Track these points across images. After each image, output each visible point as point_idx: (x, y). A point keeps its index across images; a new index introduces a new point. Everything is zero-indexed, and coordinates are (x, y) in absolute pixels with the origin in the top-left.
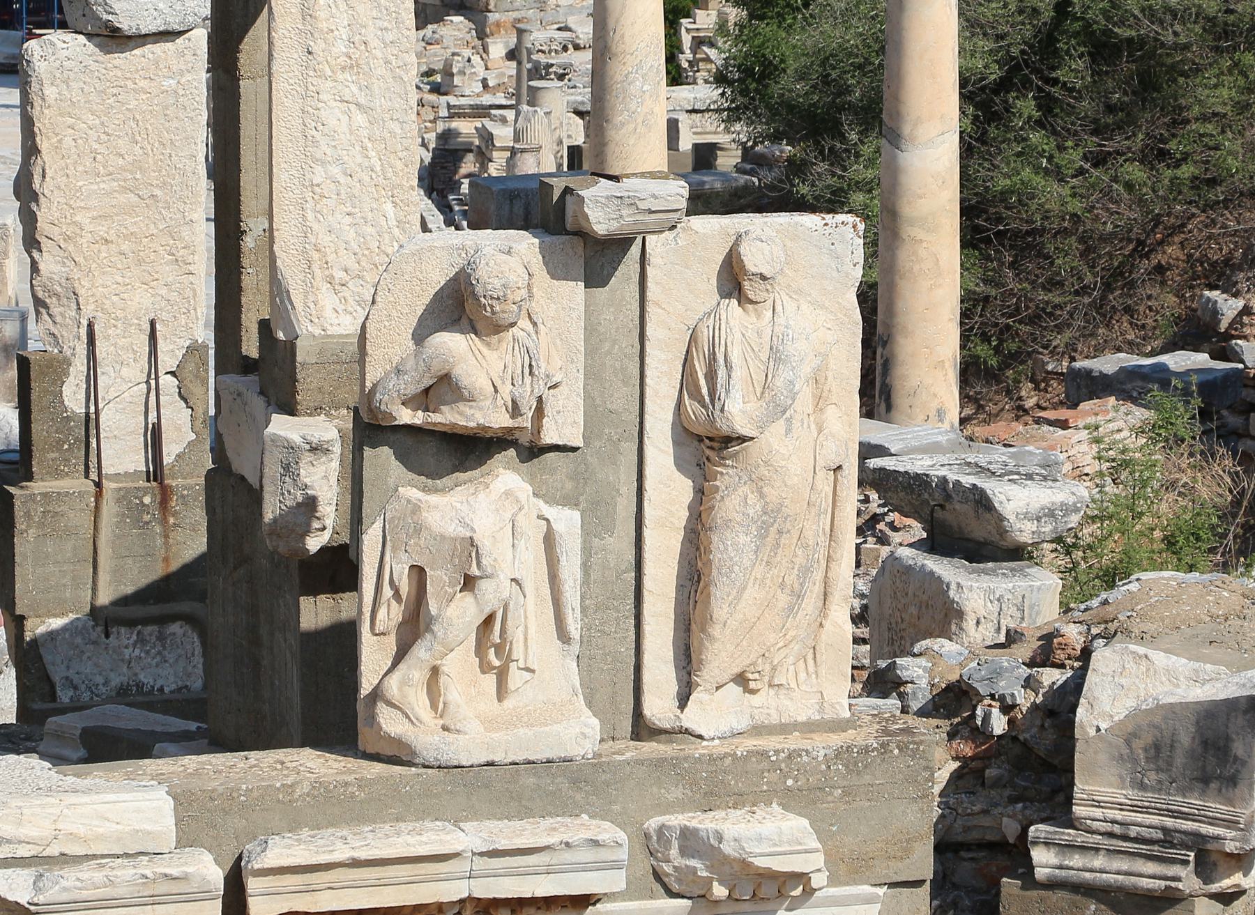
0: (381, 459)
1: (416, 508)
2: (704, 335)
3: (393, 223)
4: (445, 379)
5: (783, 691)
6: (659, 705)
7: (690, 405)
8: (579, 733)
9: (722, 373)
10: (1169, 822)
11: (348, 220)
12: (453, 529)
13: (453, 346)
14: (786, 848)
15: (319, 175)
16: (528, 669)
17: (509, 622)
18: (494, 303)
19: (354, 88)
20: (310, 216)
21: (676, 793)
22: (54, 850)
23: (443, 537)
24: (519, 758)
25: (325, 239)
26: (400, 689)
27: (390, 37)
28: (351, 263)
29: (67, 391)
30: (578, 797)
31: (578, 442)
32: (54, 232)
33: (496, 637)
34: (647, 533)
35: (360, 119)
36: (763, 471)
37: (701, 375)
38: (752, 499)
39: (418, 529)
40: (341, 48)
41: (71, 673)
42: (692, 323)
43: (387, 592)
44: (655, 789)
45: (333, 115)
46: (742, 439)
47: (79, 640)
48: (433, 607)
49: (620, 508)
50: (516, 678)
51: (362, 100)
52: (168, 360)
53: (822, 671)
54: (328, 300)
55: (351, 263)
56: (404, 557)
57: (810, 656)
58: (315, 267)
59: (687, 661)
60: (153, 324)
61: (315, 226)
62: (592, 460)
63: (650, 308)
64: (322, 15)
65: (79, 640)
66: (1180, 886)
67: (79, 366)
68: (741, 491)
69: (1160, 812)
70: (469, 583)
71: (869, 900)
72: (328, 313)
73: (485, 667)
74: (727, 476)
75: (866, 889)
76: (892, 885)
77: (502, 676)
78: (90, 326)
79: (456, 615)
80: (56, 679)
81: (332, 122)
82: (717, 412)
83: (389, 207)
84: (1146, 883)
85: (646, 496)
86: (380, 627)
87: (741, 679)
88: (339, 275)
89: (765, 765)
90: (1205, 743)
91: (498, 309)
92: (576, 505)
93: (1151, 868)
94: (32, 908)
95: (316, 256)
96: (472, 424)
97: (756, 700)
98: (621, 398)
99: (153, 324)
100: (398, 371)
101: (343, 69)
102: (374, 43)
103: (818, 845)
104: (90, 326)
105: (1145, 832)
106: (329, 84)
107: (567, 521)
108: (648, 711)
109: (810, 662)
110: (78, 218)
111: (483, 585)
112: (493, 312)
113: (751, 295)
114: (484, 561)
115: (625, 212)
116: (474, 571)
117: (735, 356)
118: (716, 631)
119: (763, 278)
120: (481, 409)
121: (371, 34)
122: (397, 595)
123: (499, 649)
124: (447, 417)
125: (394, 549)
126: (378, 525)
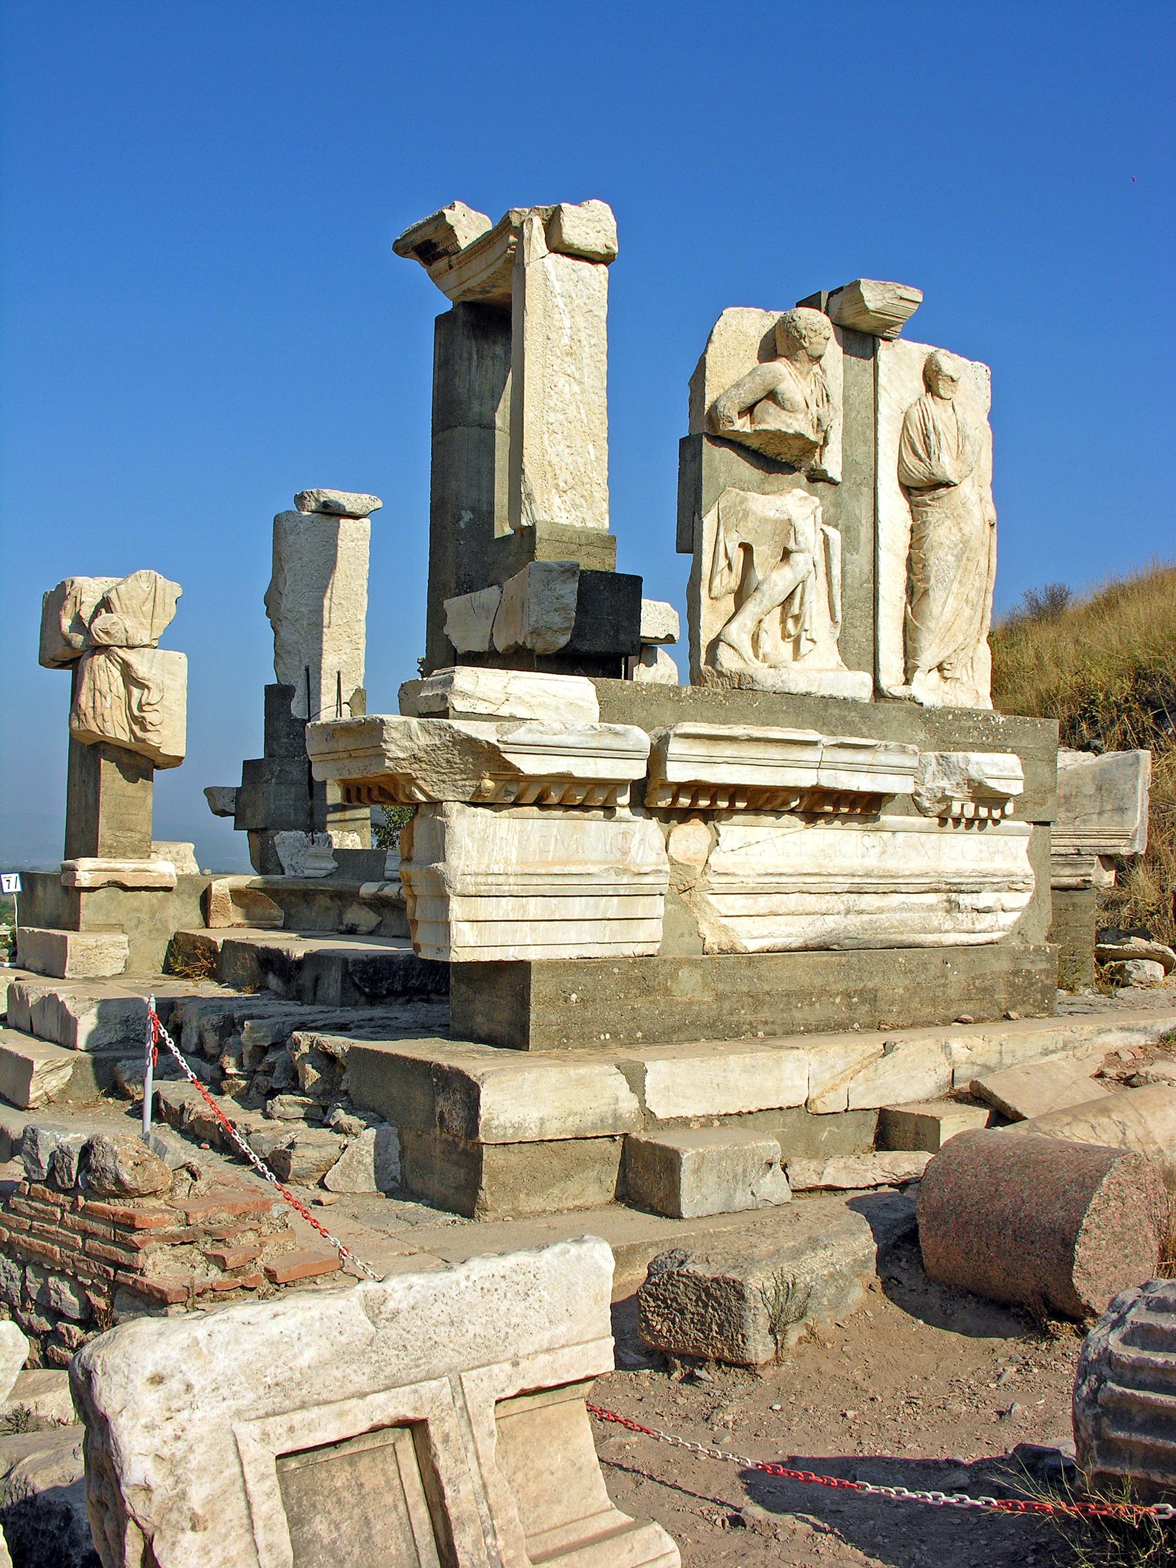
0: (718, 461)
1: (743, 500)
2: (916, 415)
3: (593, 458)
4: (772, 396)
5: (958, 685)
6: (891, 680)
7: (910, 459)
8: (858, 685)
9: (933, 437)
10: (1077, 842)
11: (568, 450)
12: (772, 514)
13: (780, 366)
14: (1005, 774)
15: (552, 417)
16: (812, 640)
17: (806, 597)
18: (812, 334)
19: (573, 367)
20: (546, 443)
21: (922, 736)
22: (504, 711)
23: (766, 520)
24: (827, 693)
25: (555, 460)
26: (738, 634)
27: (593, 342)
28: (570, 480)
29: (293, 704)
30: (864, 730)
31: (839, 478)
32: (289, 615)
33: (795, 610)
34: (881, 553)
35: (576, 388)
36: (961, 511)
37: (919, 440)
38: (955, 530)
39: (746, 514)
40: (566, 340)
41: (293, 863)
42: (905, 409)
43: (722, 562)
44: (909, 731)
45: (561, 381)
46: (948, 485)
47: (297, 844)
48: (759, 573)
49: (862, 534)
50: (805, 646)
51: (577, 376)
52: (346, 697)
53: (976, 675)
54: (557, 501)
55: (570, 480)
56: (735, 536)
57: (969, 665)
58: (549, 476)
59: (909, 653)
60: (339, 673)
61: (549, 450)
62: (845, 495)
63: (880, 390)
64: (557, 316)
65: (297, 844)
66: (1091, 878)
67: (300, 693)
68: (948, 523)
69: (1070, 836)
70: (786, 554)
71: (1022, 834)
72: (555, 508)
73: (785, 635)
74: (934, 515)
75: (1023, 824)
76: (1035, 823)
77: (797, 642)
78: (307, 670)
79: (776, 581)
80: (285, 865)
81: (560, 385)
82: (933, 463)
83: (590, 447)
84: (1066, 881)
85: (880, 526)
86: (714, 593)
87: (940, 668)
88: (562, 484)
89: (971, 723)
90: (1099, 789)
91: (813, 340)
92: (836, 526)
93: (1068, 871)
94: (501, 746)
95: (549, 469)
96: (791, 431)
97: (946, 687)
98: (861, 453)
99: (339, 673)
100: (737, 385)
101: (567, 354)
102: (585, 343)
103: (1020, 774)
104: (307, 670)
105: (1062, 851)
106: (559, 361)
107: (835, 535)
108: (884, 683)
109: (970, 669)
110: (302, 609)
111: (795, 557)
112: (811, 343)
113: (942, 392)
114: (800, 538)
115: (887, 295)
116: (792, 545)
117: (940, 427)
118: (931, 624)
119: (953, 381)
120: (797, 420)
121: (582, 336)
122: (730, 566)
123: (797, 618)
124: (773, 420)
125: (726, 531)
126: (714, 512)
